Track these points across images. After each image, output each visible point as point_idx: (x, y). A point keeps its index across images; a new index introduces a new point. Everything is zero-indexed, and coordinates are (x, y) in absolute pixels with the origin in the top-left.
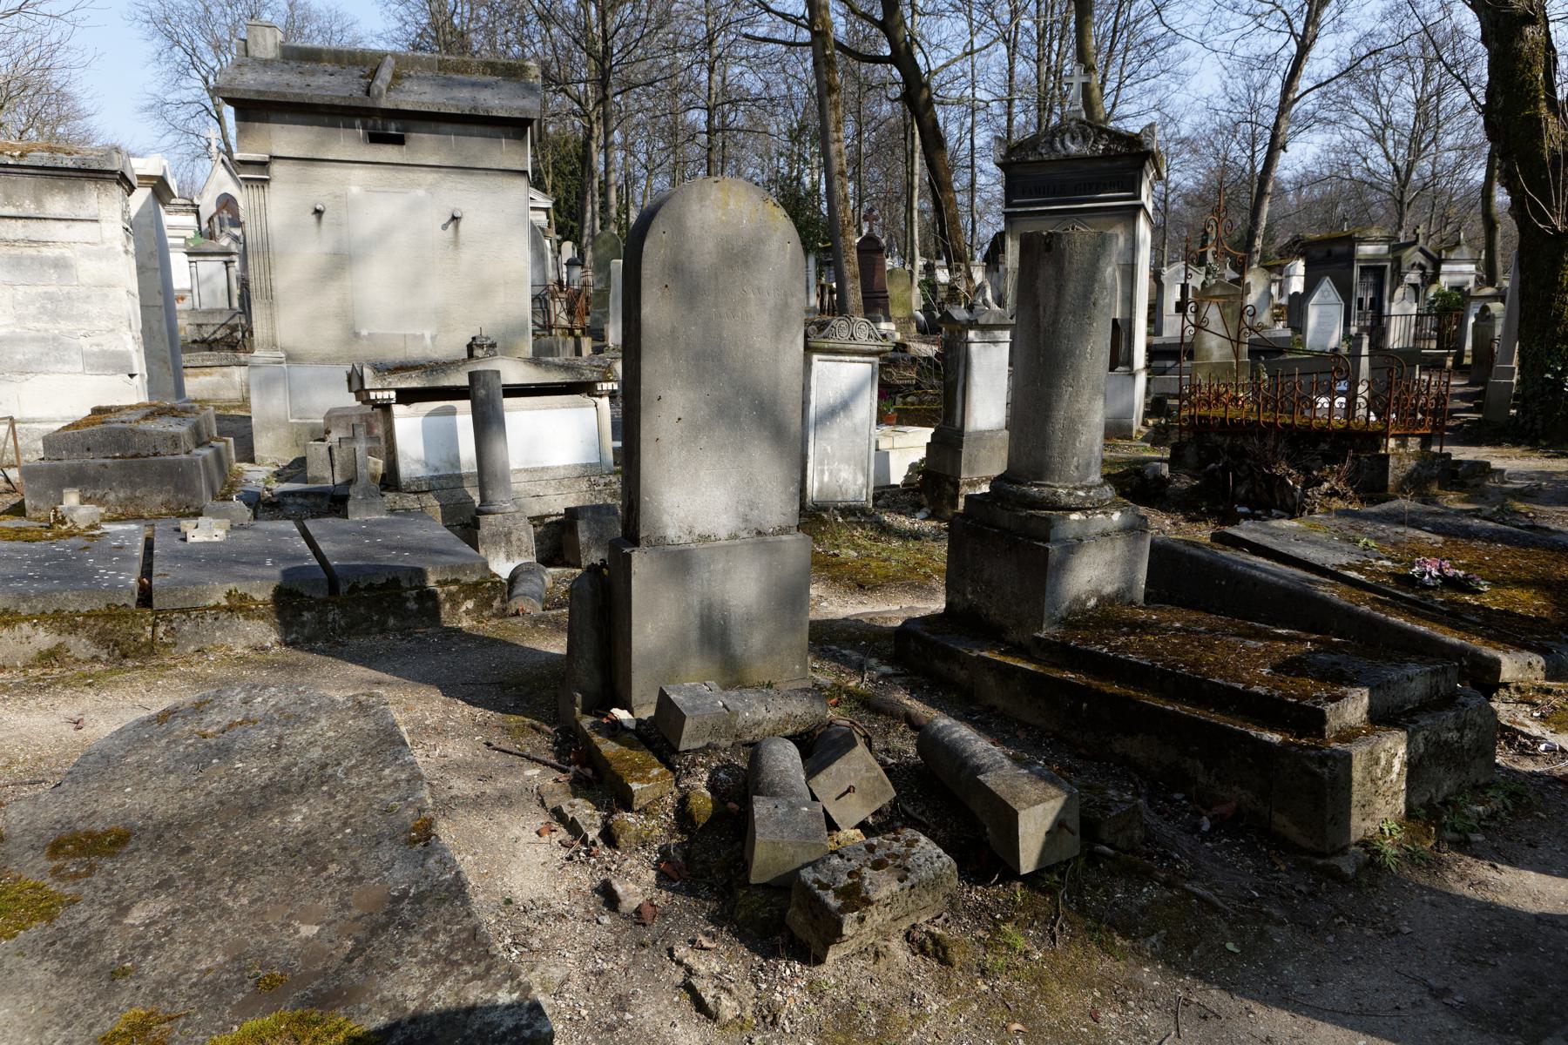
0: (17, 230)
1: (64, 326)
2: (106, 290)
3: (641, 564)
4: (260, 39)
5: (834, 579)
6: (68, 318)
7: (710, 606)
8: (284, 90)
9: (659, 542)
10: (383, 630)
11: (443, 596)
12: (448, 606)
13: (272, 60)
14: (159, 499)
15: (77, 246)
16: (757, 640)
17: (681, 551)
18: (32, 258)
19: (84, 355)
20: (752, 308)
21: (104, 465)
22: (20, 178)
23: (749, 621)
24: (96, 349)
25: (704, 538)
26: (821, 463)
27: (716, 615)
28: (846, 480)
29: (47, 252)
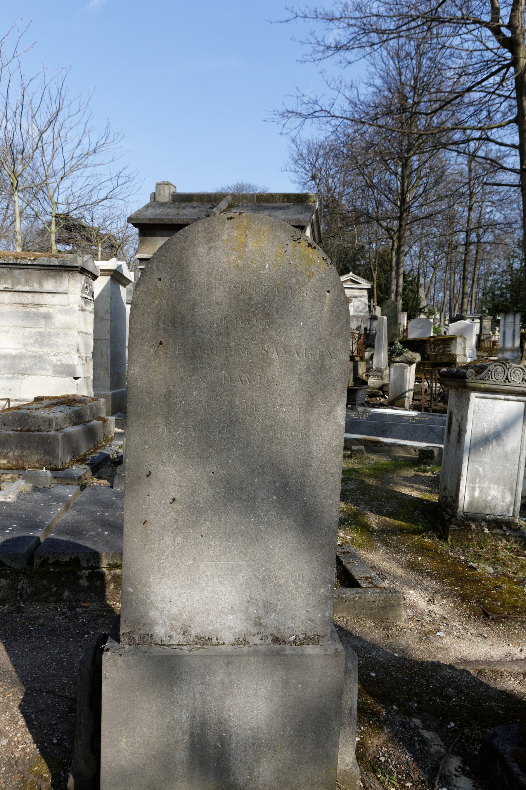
0: (29, 298)
1: (45, 350)
2: (67, 331)
3: (116, 670)
4: (162, 192)
5: (464, 598)
6: (48, 345)
7: (203, 725)
8: (163, 217)
9: (145, 641)
10: (59, 600)
11: (109, 578)
12: (112, 586)
13: (167, 203)
14: (36, 458)
15: (56, 307)
16: (266, 770)
17: (167, 658)
18: (34, 313)
19: (54, 366)
20: (276, 369)
21: (9, 435)
22: (33, 271)
23: (256, 745)
24: (59, 363)
25: (204, 641)
26: (473, 481)
27: (212, 735)
28: (494, 498)
29: (43, 310)
